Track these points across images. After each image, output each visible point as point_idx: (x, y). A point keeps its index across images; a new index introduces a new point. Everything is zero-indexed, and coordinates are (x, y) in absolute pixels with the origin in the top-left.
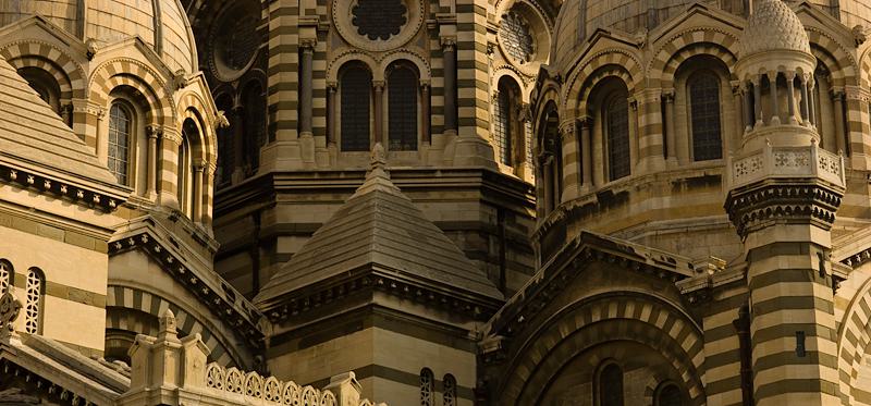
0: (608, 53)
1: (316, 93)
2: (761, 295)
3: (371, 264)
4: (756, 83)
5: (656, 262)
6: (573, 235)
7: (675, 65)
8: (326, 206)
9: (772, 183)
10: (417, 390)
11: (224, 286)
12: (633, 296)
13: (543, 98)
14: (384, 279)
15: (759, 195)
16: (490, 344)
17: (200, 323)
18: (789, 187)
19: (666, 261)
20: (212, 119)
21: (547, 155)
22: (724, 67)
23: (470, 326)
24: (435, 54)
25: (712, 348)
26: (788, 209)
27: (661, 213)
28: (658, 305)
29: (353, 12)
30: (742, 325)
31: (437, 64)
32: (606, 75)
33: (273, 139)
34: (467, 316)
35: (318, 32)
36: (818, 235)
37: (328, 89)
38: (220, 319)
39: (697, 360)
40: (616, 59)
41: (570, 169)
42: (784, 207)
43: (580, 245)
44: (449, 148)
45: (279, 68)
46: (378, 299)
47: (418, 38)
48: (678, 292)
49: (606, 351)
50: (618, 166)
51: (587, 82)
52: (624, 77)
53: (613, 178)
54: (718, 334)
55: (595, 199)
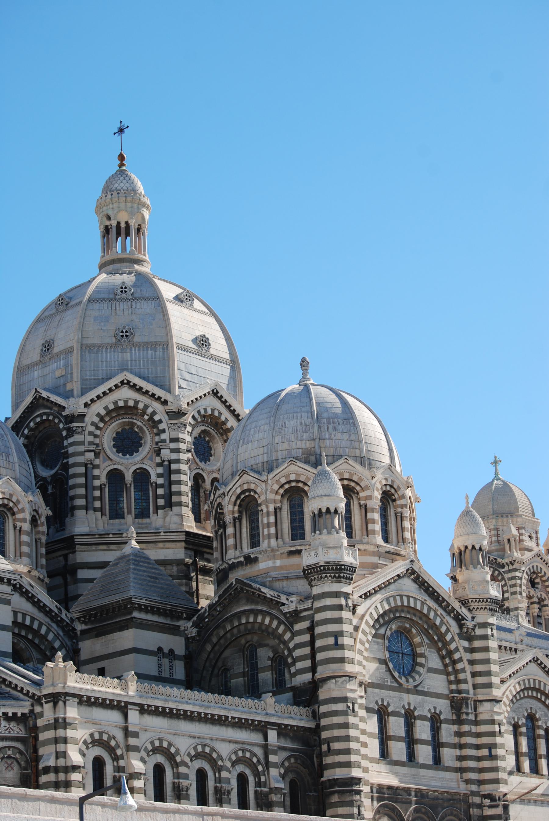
0: (248, 483)
1: (94, 488)
2: (318, 617)
3: (131, 598)
4: (316, 512)
5: (271, 596)
7: (281, 491)
8: (103, 552)
9: (323, 564)
10: (155, 658)
11: (56, 606)
12: (261, 612)
13: (216, 500)
14: (138, 604)
15: (317, 570)
16: (191, 633)
17: (45, 625)
18: (330, 565)
19: (276, 596)
20: (45, 511)
21: (219, 530)
23: (181, 623)
25: (298, 639)
26: (330, 576)
27: (275, 568)
28: (273, 617)
29: (114, 440)
30: (311, 629)
31: (160, 470)
32: (247, 494)
33: (73, 515)
34: (179, 618)
35: (95, 454)
36: (347, 589)
37: (101, 485)
38: (54, 622)
39: (291, 645)
40: (252, 486)
41: (231, 542)
42: (328, 575)
43: (235, 585)
44: (168, 519)
45: (75, 476)
46: (136, 614)
47: (149, 455)
48: (281, 611)
49: (249, 637)
51: (238, 497)
52: (256, 496)
53: (252, 547)
54: (300, 633)
55: (242, 559)
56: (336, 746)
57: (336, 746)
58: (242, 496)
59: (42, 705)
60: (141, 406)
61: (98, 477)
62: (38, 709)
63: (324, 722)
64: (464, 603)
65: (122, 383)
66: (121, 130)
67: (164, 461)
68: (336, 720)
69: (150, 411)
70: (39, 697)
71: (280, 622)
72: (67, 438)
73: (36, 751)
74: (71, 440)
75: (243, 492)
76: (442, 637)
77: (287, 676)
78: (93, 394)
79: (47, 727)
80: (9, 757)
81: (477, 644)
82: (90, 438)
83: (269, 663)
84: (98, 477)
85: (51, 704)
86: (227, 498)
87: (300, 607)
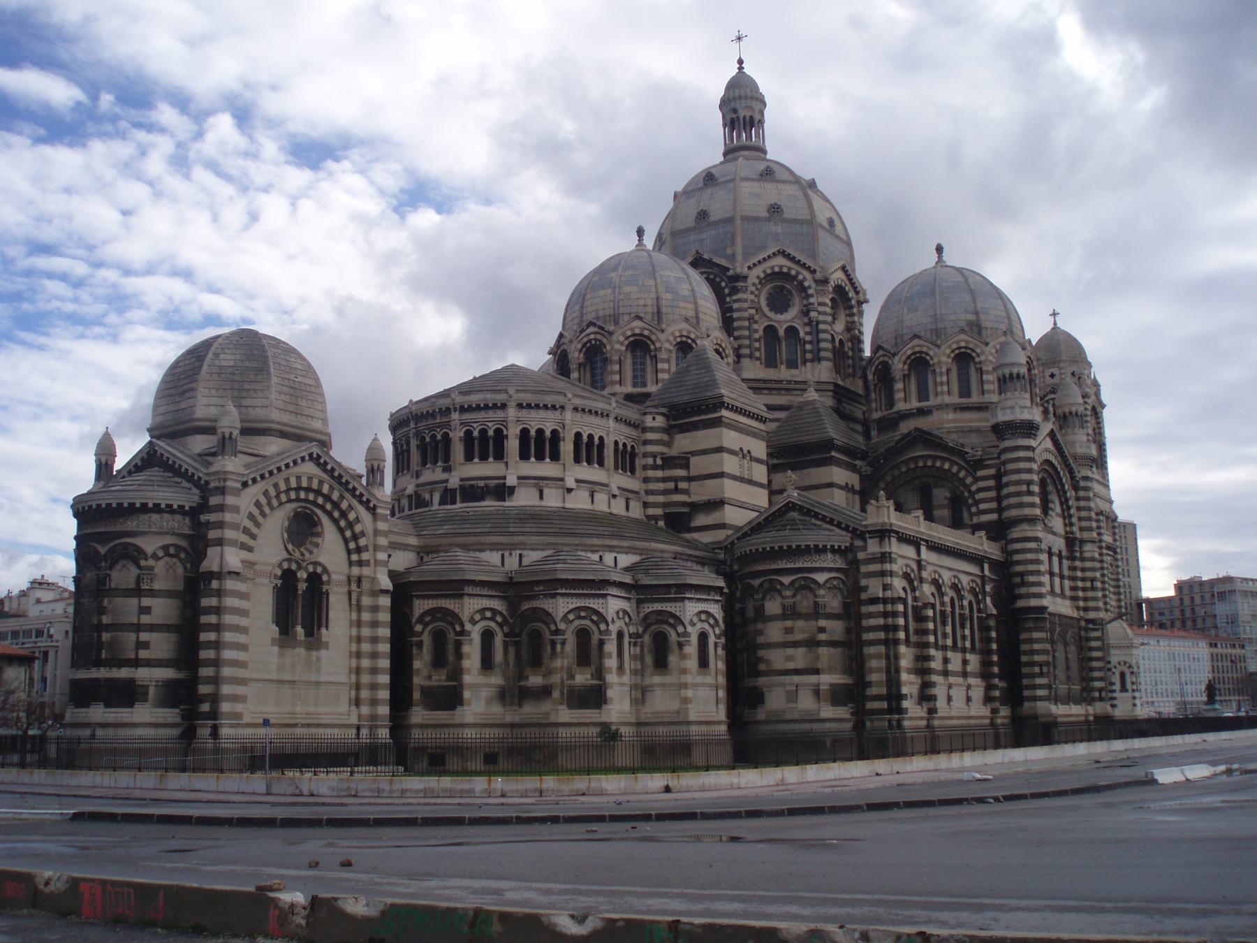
6: (906, 427)
16: (866, 471)
22: (973, 359)
24: (805, 324)
25: (981, 484)
27: (949, 421)
28: (953, 463)
30: (998, 477)
36: (1033, 443)
40: (924, 349)
41: (899, 395)
45: (739, 328)
46: (833, 454)
50: (923, 395)
51: (909, 357)
52: (928, 358)
56: (1031, 579)
57: (1031, 579)
59: (865, 540)
61: (756, 331)
62: (858, 543)
63: (1016, 557)
64: (1075, 457)
65: (779, 251)
66: (739, 38)
68: (1030, 556)
70: (863, 533)
71: (961, 468)
72: (730, 295)
73: (857, 582)
74: (735, 297)
75: (914, 353)
76: (1063, 486)
77: (966, 515)
79: (870, 561)
80: (835, 587)
81: (1081, 493)
82: (752, 297)
83: (946, 502)
84: (756, 331)
85: (877, 539)
86: (897, 358)
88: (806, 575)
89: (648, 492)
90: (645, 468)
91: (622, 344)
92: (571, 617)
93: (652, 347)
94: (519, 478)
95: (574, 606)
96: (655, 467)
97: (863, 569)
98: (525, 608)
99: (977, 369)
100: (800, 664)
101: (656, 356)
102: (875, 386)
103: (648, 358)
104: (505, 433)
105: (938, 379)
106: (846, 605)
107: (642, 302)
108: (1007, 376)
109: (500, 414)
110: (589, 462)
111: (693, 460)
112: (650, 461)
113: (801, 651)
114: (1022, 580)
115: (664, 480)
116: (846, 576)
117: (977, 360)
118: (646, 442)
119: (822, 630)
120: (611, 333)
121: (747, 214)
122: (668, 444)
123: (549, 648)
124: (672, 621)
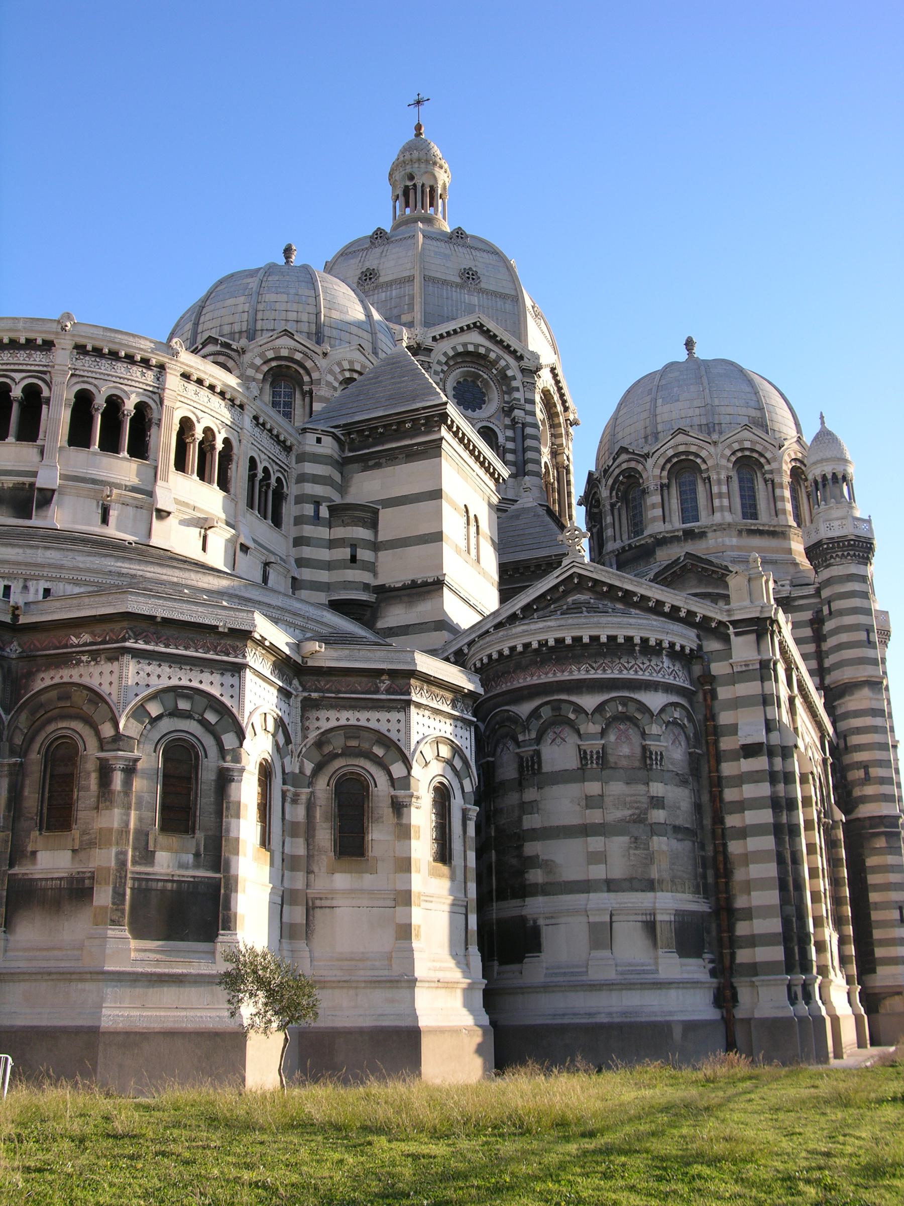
9: (853, 537)
15: (844, 544)
22: (762, 466)
24: (507, 427)
27: (732, 548)
40: (693, 449)
51: (669, 460)
52: (699, 461)
55: (681, 533)
57: (875, 772)
58: (675, 460)
59: (726, 639)
60: (492, 356)
62: (711, 645)
63: (855, 740)
65: (475, 324)
66: (418, 103)
67: (517, 423)
69: (502, 363)
73: (711, 716)
75: (676, 455)
78: (443, 329)
79: (735, 678)
80: (675, 723)
86: (650, 462)
87: (795, 594)
88: (626, 694)
89: (301, 563)
90: (299, 520)
91: (258, 369)
92: (154, 709)
93: (306, 379)
94: (64, 477)
95: (165, 683)
96: (316, 519)
97: (724, 693)
98: (39, 685)
99: (766, 481)
100: (617, 868)
101: (311, 392)
102: (613, 506)
103: (298, 395)
104: (46, 393)
105: (715, 489)
106: (694, 761)
107: (293, 316)
108: (829, 477)
109: (38, 358)
110: (202, 475)
111: (385, 515)
112: (309, 509)
113: (617, 844)
114: (867, 773)
115: (332, 544)
116: (691, 702)
117: (767, 467)
118: (302, 478)
119: (657, 802)
120: (243, 352)
121: (433, 274)
122: (342, 489)
123: (93, 782)
124: (379, 751)
